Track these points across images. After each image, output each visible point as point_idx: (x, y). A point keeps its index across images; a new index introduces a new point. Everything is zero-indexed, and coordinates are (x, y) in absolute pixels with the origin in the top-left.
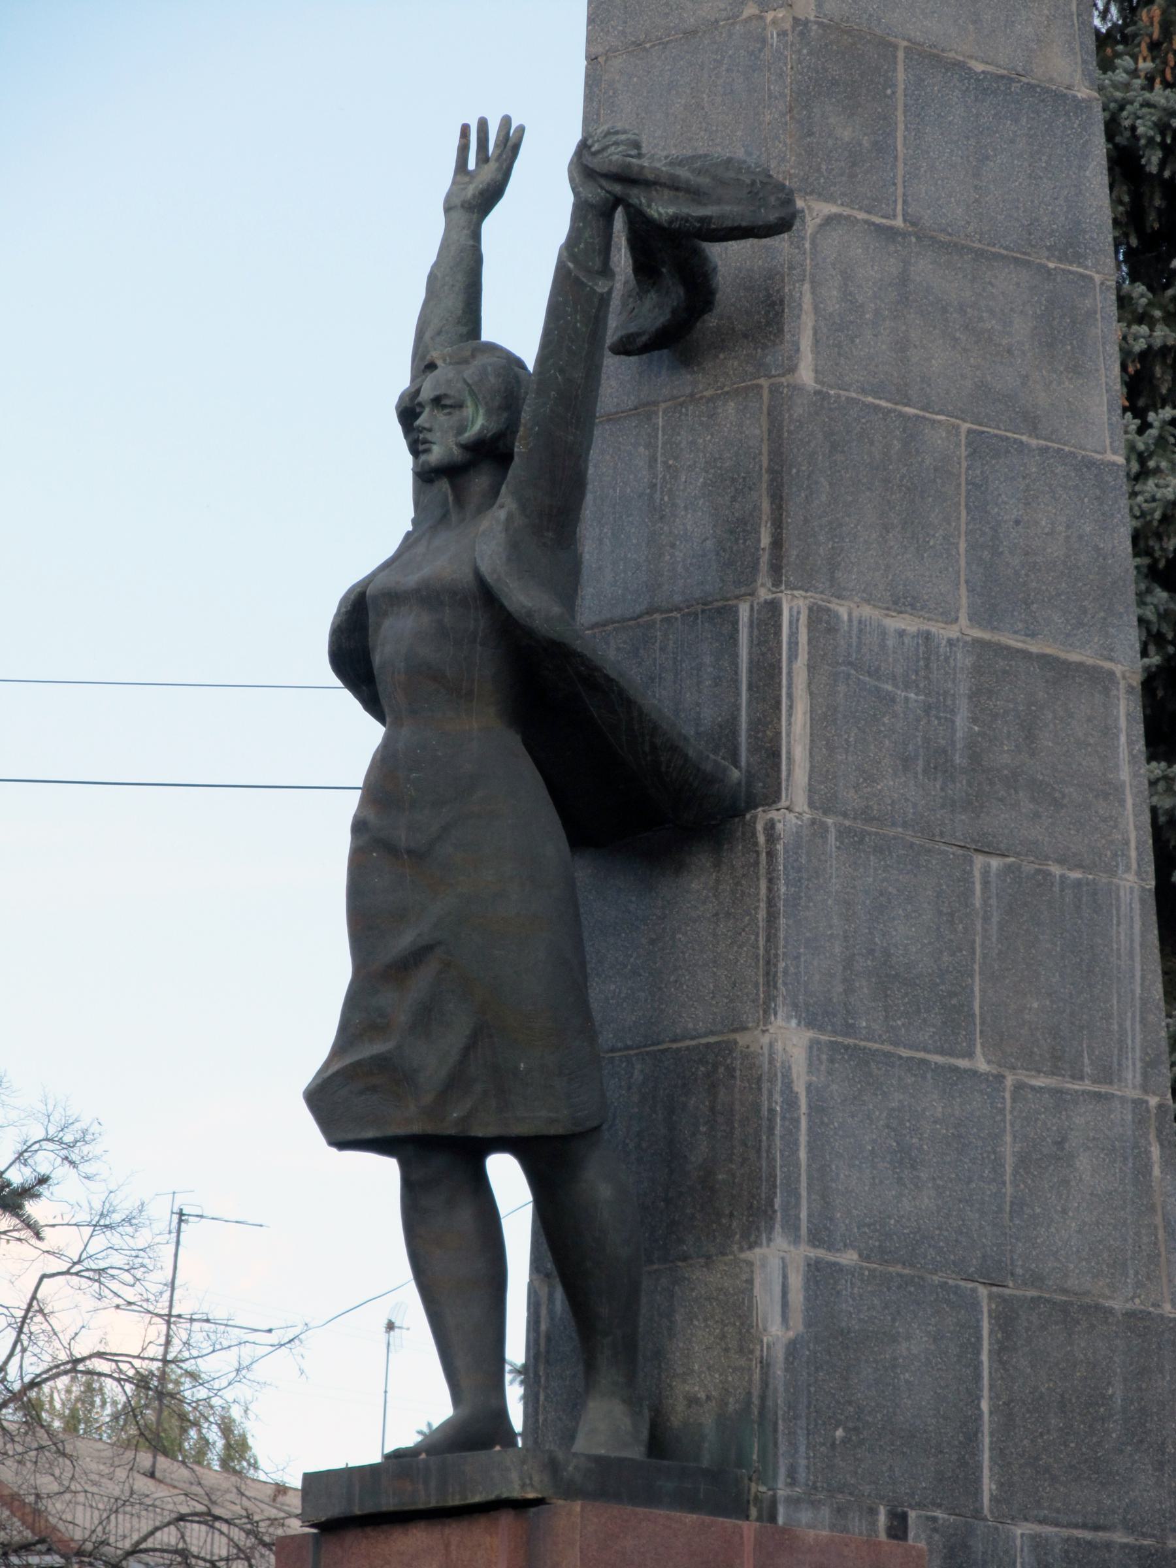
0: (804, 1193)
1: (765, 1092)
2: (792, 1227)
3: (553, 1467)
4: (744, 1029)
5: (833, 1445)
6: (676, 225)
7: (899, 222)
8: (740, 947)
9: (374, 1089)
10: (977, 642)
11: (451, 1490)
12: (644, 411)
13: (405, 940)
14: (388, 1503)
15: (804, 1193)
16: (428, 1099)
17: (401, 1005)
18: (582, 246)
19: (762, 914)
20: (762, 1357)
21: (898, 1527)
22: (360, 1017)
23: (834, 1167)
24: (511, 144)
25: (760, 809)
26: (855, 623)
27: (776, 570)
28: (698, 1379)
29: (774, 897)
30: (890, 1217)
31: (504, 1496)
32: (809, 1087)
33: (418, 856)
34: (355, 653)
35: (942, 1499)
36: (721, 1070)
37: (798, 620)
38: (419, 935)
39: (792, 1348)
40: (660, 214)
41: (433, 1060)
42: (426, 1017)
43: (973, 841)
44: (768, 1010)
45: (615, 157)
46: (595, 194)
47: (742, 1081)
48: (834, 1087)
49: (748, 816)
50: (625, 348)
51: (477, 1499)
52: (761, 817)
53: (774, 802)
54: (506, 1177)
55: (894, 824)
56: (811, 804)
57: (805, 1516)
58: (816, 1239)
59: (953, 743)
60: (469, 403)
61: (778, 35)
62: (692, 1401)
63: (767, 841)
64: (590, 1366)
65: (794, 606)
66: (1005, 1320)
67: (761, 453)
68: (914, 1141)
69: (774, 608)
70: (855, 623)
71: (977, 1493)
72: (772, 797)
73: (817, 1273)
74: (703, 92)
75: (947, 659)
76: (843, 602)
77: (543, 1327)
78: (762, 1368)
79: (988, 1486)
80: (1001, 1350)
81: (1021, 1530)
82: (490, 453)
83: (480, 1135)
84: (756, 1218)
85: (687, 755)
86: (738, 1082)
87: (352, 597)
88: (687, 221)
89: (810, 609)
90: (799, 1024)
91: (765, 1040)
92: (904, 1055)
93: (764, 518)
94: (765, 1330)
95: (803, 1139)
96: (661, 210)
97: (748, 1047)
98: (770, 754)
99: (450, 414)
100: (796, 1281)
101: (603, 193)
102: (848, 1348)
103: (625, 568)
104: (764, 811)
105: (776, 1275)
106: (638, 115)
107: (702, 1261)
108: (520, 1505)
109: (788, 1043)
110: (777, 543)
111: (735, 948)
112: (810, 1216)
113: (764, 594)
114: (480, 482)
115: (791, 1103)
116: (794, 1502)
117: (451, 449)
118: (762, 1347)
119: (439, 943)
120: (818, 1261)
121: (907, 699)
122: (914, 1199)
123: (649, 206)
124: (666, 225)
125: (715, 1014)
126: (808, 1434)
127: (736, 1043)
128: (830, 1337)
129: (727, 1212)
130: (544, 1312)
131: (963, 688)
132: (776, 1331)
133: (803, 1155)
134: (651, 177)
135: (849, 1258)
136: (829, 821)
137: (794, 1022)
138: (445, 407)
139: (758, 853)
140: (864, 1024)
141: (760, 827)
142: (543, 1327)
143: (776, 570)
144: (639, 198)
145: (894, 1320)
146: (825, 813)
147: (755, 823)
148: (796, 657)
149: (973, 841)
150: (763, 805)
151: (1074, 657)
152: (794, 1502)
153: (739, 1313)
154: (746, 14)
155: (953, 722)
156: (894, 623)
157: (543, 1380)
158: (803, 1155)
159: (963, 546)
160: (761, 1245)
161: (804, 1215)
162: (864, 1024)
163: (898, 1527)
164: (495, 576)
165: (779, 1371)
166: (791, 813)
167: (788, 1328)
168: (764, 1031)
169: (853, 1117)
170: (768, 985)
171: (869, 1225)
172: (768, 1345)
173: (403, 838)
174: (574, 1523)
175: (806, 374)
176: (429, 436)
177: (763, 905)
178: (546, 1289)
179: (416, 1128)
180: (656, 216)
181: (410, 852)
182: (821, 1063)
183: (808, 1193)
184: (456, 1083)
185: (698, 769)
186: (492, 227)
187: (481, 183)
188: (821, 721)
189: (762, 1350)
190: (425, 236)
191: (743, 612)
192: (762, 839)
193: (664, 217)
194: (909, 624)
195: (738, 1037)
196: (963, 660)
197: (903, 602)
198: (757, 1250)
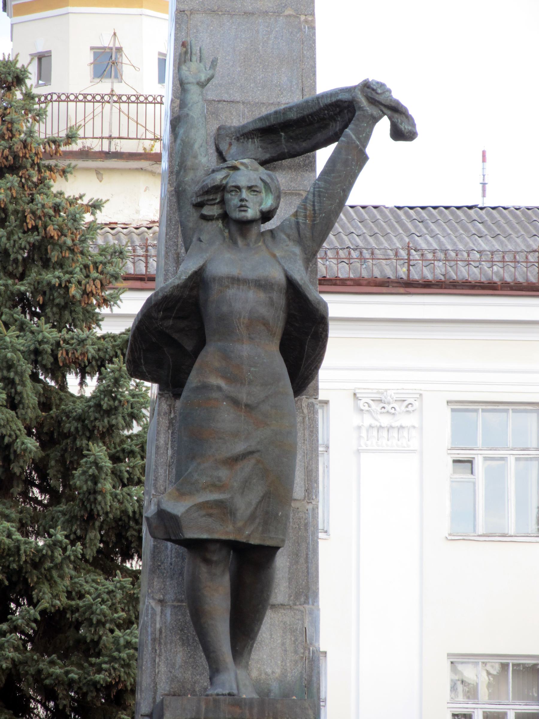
9: (210, 515)
11: (267, 715)
18: (364, 135)
20: (309, 656)
38: (250, 446)
40: (405, 129)
53: (314, 395)
60: (263, 191)
61: (308, 28)
74: (259, 44)
77: (158, 626)
78: (309, 662)
86: (291, 524)
91: (310, 507)
94: (311, 644)
96: (406, 127)
97: (298, 508)
99: (256, 195)
104: (307, 398)
106: (214, 46)
117: (256, 215)
118: (309, 652)
119: (258, 451)
123: (401, 124)
130: (158, 618)
138: (254, 191)
142: (158, 626)
144: (397, 119)
150: (306, 395)
154: (287, 13)
157: (158, 651)
160: (308, 603)
164: (303, 282)
168: (308, 503)
172: (313, 651)
173: (245, 398)
176: (247, 204)
179: (231, 537)
180: (403, 129)
181: (247, 406)
193: (406, 131)
198: (306, 606)
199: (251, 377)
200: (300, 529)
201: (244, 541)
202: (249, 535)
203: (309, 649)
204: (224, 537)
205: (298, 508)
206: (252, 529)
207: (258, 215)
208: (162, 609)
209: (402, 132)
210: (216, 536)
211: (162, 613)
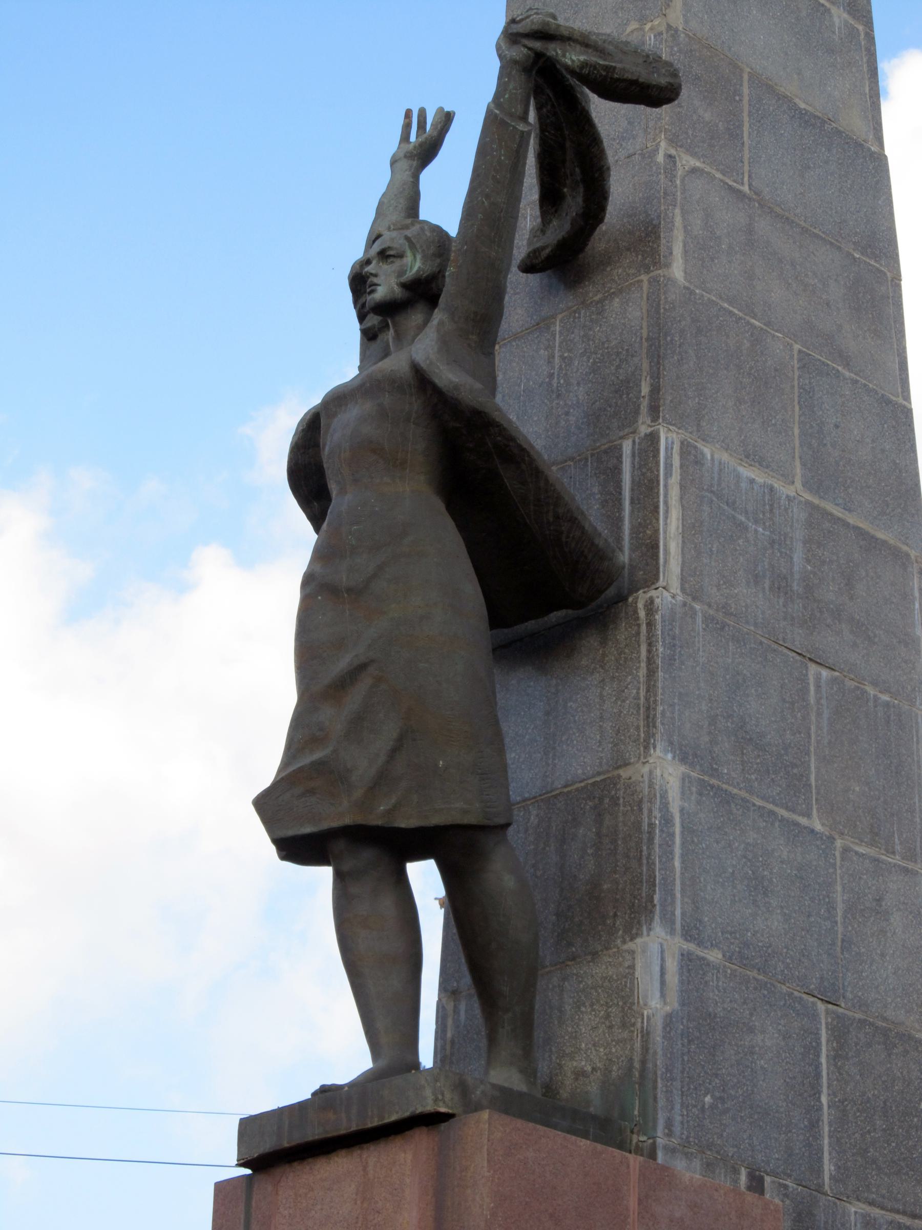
0: (678, 895)
1: (645, 812)
2: (669, 921)
3: (462, 1088)
4: (626, 764)
5: (703, 1109)
6: (586, 71)
7: (746, 189)
8: (624, 701)
9: (311, 792)
10: (808, 503)
11: (370, 1113)
12: (542, 325)
13: (343, 663)
14: (314, 1133)
15: (678, 895)
16: (358, 794)
17: (334, 718)
18: (507, 96)
19: (643, 672)
20: (643, 1027)
21: (756, 1184)
22: (304, 733)
23: (702, 879)
24: (446, 119)
25: (641, 591)
26: (716, 463)
27: (654, 411)
28: (583, 1052)
29: (653, 657)
30: (747, 931)
31: (420, 1110)
32: (682, 810)
33: (356, 593)
34: (310, 477)
35: (791, 1170)
36: (607, 800)
37: (672, 448)
38: (356, 656)
39: (669, 1020)
40: (573, 61)
41: (363, 762)
42: (358, 725)
43: (808, 651)
44: (647, 746)
45: (535, 21)
46: (518, 53)
47: (624, 806)
48: (702, 815)
49: (630, 600)
50: (529, 267)
51: (394, 1118)
52: (641, 598)
53: (653, 583)
54: (425, 879)
55: (747, 622)
56: (683, 590)
57: (680, 1165)
58: (687, 935)
59: (792, 574)
60: (409, 254)
62: (580, 1074)
63: (647, 615)
64: (492, 1039)
65: (669, 438)
66: (840, 1031)
67: (641, 328)
68: (766, 873)
69: (653, 438)
70: (716, 463)
71: (819, 1172)
72: (652, 578)
73: (688, 962)
75: (786, 510)
76: (708, 445)
77: (449, 1035)
78: (642, 1036)
79: (828, 1168)
80: (836, 1057)
81: (855, 1209)
82: (423, 292)
83: (403, 826)
84: (639, 913)
85: (584, 528)
86: (622, 808)
87: (308, 417)
88: (595, 68)
89: (682, 443)
90: (674, 758)
91: (646, 769)
92: (757, 803)
93: (645, 374)
94: (645, 1005)
95: (677, 851)
96: (574, 58)
97: (630, 778)
98: (650, 548)
100: (672, 965)
101: (525, 51)
102: (714, 1029)
103: (534, 380)
105: (655, 962)
107: (589, 958)
108: (432, 1120)
109: (664, 773)
110: (655, 390)
111: (619, 703)
112: (683, 914)
113: (644, 430)
114: (415, 317)
115: (667, 821)
116: (671, 1151)
117: (393, 288)
118: (643, 1019)
119: (372, 661)
120: (689, 954)
121: (756, 531)
122: (767, 919)
123: (564, 56)
124: (578, 70)
125: (601, 758)
126: (682, 1095)
127: (619, 776)
128: (700, 1023)
129: (611, 914)
130: (450, 1022)
131: (799, 534)
132: (656, 1000)
133: (677, 863)
134: (566, 33)
135: (714, 956)
136: (697, 607)
137: (670, 756)
139: (639, 626)
140: (726, 771)
141: (640, 605)
142: (449, 1035)
143: (654, 411)
145: (751, 1015)
146: (694, 599)
147: (636, 603)
148: (671, 475)
149: (808, 651)
151: (881, 535)
152: (671, 1151)
153: (623, 994)
155: (792, 558)
156: (746, 472)
158: (677, 863)
159: (797, 431)
161: (678, 912)
162: (726, 771)
163: (756, 1184)
165: (658, 1037)
166: (668, 593)
167: (665, 1003)
168: (644, 763)
169: (717, 843)
170: (648, 726)
171: (731, 933)
172: (648, 1017)
173: (344, 580)
174: (483, 1131)
175: (677, 270)
176: (375, 280)
177: (643, 665)
178: (452, 1004)
179: (347, 821)
180: (569, 62)
181: (349, 590)
182: (692, 794)
183: (682, 896)
184: (382, 781)
185: (593, 544)
186: (427, 177)
187: (423, 149)
188: (690, 530)
189: (643, 1022)
190: (377, 179)
191: (627, 447)
192: (642, 614)
193: (577, 63)
195: (621, 772)
196: (799, 515)
197: (752, 457)
198: (639, 940)
199: (354, 542)
200: (632, 810)
201: (379, 822)
202: (389, 812)
203: (643, 1015)
204: (335, 824)
205: (630, 778)
206: (393, 801)
207: (398, 292)
208: (455, 1006)
209: (648, 91)
210: (325, 825)
211: (454, 1011)
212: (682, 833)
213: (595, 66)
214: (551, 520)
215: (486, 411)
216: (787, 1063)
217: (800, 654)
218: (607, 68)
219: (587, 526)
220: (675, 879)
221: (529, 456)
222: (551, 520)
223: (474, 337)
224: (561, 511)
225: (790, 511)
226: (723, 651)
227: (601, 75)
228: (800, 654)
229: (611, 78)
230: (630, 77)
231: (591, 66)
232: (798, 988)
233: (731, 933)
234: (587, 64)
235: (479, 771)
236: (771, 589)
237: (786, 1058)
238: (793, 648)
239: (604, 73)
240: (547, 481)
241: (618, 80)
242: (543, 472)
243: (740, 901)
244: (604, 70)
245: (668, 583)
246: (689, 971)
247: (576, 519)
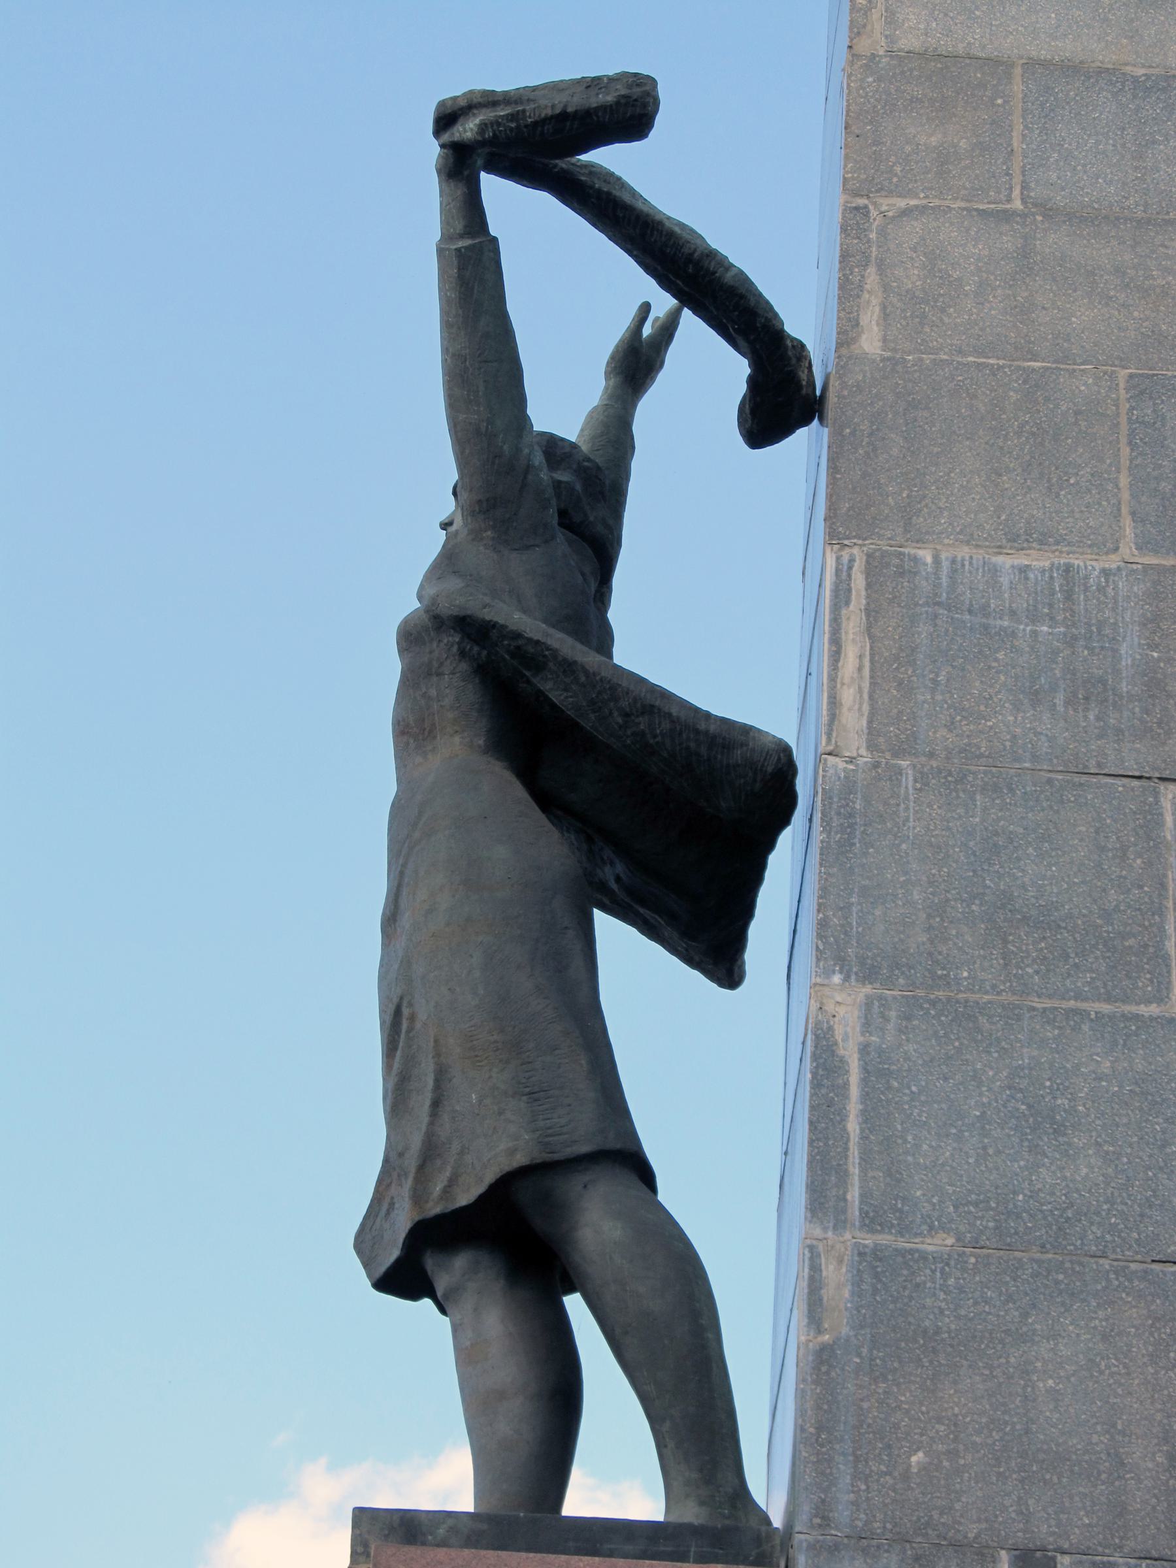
0: (855, 1170)
5: (906, 1476)
6: (489, 134)
7: (1018, 204)
10: (1147, 568)
15: (855, 1170)
23: (910, 1138)
26: (945, 565)
30: (1015, 1193)
32: (864, 1050)
35: (1121, 1538)
37: (850, 568)
43: (1154, 769)
48: (911, 1047)
55: (1017, 759)
56: (872, 746)
58: (872, 1220)
59: (1117, 672)
68: (1059, 1102)
70: (945, 565)
75: (1101, 590)
76: (926, 545)
85: (670, 714)
88: (499, 124)
89: (869, 556)
90: (847, 978)
92: (1038, 1006)
95: (854, 1106)
96: (471, 125)
102: (934, 1351)
112: (865, 1196)
121: (1035, 633)
122: (1062, 1169)
124: (480, 138)
126: (857, 1459)
133: (853, 1126)
134: (463, 103)
136: (904, 764)
137: (837, 979)
140: (965, 974)
145: (1025, 1315)
146: (896, 755)
148: (848, 603)
149: (1154, 769)
155: (1115, 651)
156: (1006, 562)
158: (853, 1126)
159: (1124, 480)
161: (854, 1194)
162: (965, 974)
167: (820, 1331)
169: (946, 1079)
171: (976, 1204)
182: (887, 1020)
183: (864, 1171)
185: (697, 732)
194: (1038, 561)
201: (437, 1210)
202: (447, 1191)
206: (448, 1174)
212: (864, 1081)
213: (497, 123)
214: (620, 720)
215: (469, 612)
216: (1112, 1374)
217: (1140, 777)
218: (513, 117)
219: (674, 711)
220: (847, 1149)
221: (548, 648)
222: (620, 720)
223: (489, 533)
224: (624, 703)
225: (1110, 591)
226: (961, 811)
227: (511, 129)
228: (1140, 777)
229: (526, 126)
230: (549, 112)
231: (492, 124)
232: (1139, 1257)
233: (976, 1204)
234: (486, 125)
235: (527, 1090)
236: (1067, 703)
237: (1108, 1367)
238: (1121, 772)
239: (513, 125)
240: (586, 672)
241: (535, 124)
242: (575, 662)
243: (998, 1152)
244: (512, 121)
245: (837, 746)
246: (876, 1276)
247: (652, 706)
